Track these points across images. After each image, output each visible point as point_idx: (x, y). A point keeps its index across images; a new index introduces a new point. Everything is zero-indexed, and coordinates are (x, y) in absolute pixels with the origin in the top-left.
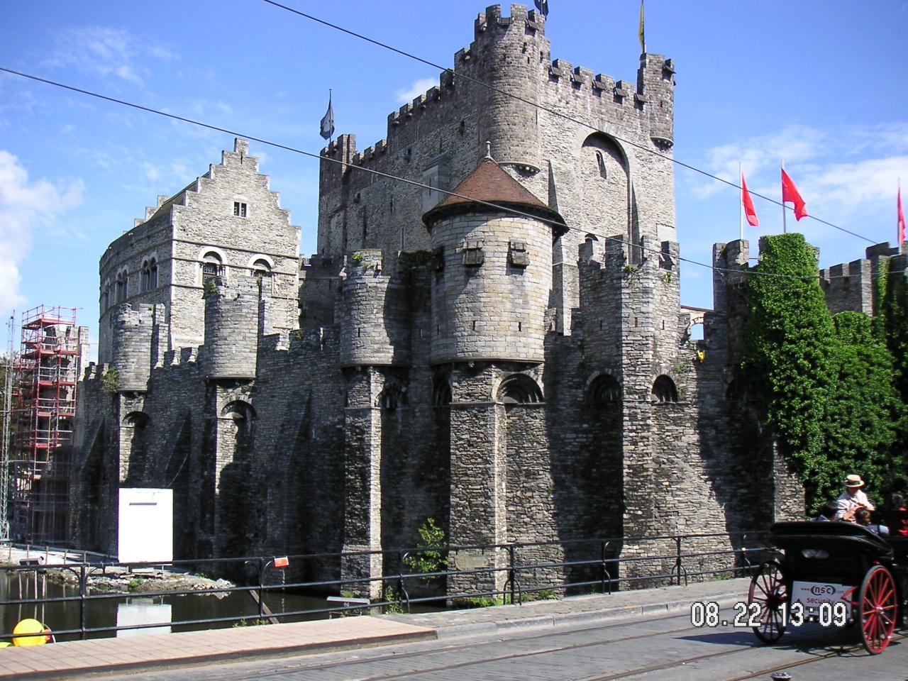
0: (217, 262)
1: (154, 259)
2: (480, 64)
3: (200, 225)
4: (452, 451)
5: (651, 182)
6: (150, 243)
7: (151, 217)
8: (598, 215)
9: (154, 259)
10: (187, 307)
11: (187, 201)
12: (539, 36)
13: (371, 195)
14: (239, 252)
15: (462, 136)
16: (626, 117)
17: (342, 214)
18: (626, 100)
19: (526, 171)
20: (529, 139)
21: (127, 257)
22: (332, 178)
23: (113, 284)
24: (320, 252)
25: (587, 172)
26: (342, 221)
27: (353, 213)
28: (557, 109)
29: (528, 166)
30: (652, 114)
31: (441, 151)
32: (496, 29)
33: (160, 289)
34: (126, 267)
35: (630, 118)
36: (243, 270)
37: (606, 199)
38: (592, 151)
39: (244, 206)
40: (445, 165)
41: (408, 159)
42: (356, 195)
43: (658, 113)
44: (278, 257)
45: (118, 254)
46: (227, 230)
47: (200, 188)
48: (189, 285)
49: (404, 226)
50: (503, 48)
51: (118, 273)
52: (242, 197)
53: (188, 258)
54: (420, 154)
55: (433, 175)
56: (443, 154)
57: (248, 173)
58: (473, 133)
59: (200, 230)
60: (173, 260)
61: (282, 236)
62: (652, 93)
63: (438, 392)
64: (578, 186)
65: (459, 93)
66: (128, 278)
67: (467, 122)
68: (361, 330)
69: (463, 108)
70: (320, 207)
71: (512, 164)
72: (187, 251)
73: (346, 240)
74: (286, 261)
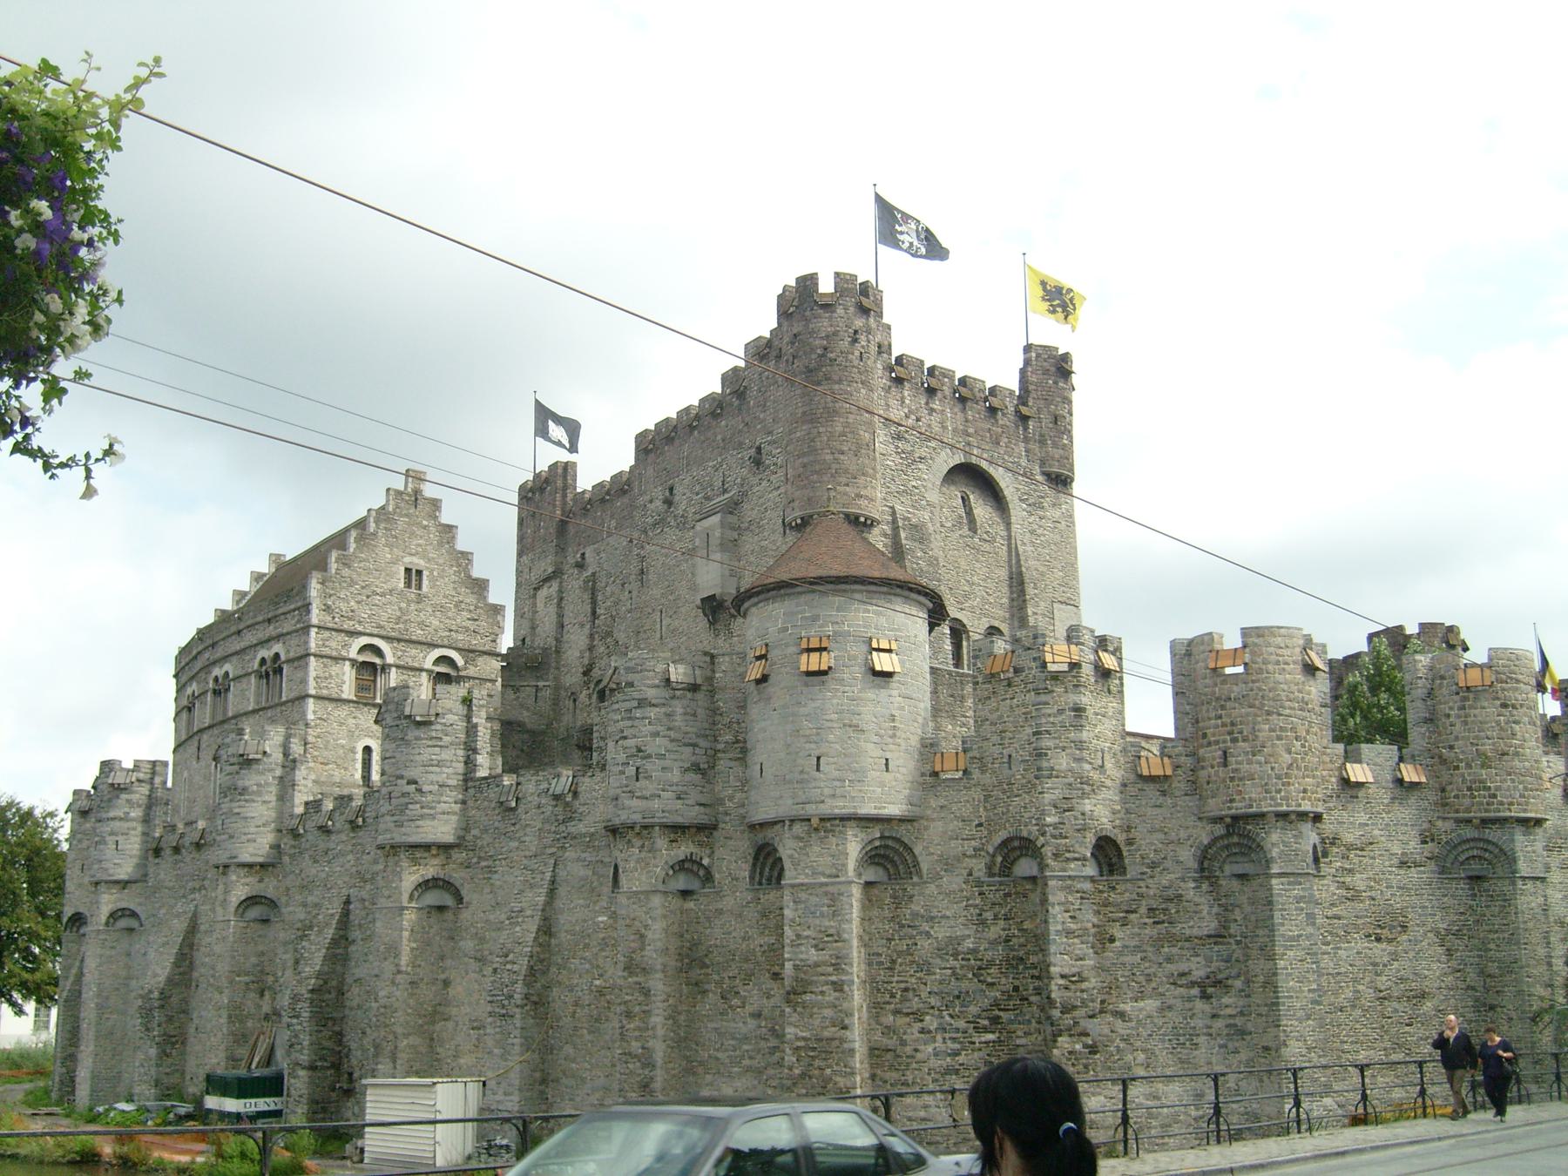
0: (377, 661)
1: (277, 656)
2: (787, 361)
3: (352, 604)
4: (786, 956)
5: (1042, 538)
6: (271, 630)
7: (258, 587)
8: (966, 588)
9: (277, 656)
10: (332, 731)
11: (333, 566)
12: (875, 320)
13: (603, 555)
14: (411, 646)
15: (758, 469)
16: (1004, 441)
17: (555, 585)
18: (1004, 414)
19: (859, 523)
20: (863, 474)
21: (230, 652)
23: (207, 691)
24: (519, 643)
25: (949, 525)
27: (574, 583)
28: (902, 428)
29: (863, 515)
30: (1042, 435)
31: (725, 491)
32: (812, 310)
33: (287, 702)
34: (227, 667)
35: (1010, 442)
37: (978, 565)
38: (955, 493)
39: (419, 573)
40: (731, 513)
41: (669, 502)
42: (579, 555)
43: (1052, 434)
44: (468, 652)
45: (213, 645)
46: (392, 611)
47: (352, 546)
48: (335, 696)
51: (214, 674)
52: (415, 560)
53: (334, 654)
56: (726, 496)
57: (425, 523)
59: (352, 611)
60: (312, 658)
62: (1041, 404)
63: (759, 864)
64: (936, 544)
66: (232, 684)
67: (766, 448)
68: (640, 770)
69: (759, 426)
70: (519, 573)
72: (333, 644)
73: (561, 626)
74: (481, 660)
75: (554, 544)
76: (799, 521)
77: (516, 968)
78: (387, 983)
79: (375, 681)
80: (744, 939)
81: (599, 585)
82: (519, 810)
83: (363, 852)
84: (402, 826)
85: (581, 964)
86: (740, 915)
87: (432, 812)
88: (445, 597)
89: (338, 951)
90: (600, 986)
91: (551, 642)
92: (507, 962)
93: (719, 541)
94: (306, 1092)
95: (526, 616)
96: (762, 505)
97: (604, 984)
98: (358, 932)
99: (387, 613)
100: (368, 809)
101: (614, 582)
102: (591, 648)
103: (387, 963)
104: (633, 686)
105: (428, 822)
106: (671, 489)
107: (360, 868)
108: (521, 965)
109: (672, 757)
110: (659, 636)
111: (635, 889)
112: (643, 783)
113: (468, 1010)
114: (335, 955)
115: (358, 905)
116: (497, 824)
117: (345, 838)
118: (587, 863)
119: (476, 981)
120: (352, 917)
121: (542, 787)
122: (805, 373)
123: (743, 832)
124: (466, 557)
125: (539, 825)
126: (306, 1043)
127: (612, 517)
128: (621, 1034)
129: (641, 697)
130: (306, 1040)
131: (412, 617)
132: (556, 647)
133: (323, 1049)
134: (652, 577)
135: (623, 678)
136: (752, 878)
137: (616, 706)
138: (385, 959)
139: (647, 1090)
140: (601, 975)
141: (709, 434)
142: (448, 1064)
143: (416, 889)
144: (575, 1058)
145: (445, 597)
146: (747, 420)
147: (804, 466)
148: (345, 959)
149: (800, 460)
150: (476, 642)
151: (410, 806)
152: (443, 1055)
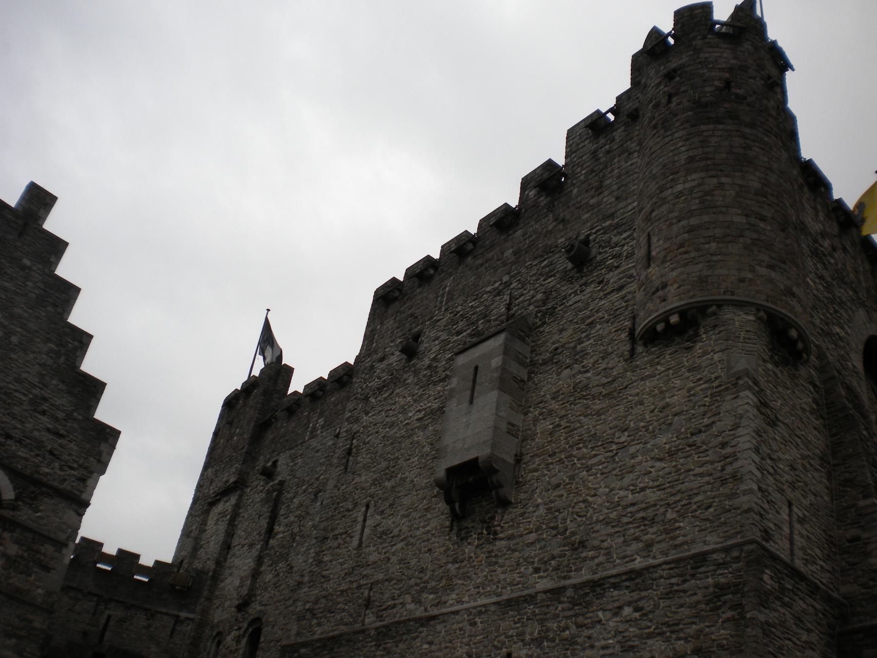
15: (580, 271)
17: (233, 500)
22: (232, 438)
26: (230, 509)
29: (798, 327)
42: (269, 464)
49: (372, 496)
50: (722, 70)
54: (444, 336)
57: (27, 262)
58: (617, 256)
61: (61, 436)
65: (575, 191)
70: (200, 487)
71: (759, 308)
73: (227, 547)
75: (244, 450)
88: (18, 380)
91: (211, 565)
93: (496, 375)
95: (193, 535)
96: (583, 320)
101: (305, 491)
102: (256, 574)
106: (416, 337)
110: (355, 542)
124: (82, 340)
127: (320, 416)
132: (215, 571)
134: (363, 458)
145: (18, 380)
146: (561, 217)
147: (691, 230)
149: (684, 223)
150: (48, 470)
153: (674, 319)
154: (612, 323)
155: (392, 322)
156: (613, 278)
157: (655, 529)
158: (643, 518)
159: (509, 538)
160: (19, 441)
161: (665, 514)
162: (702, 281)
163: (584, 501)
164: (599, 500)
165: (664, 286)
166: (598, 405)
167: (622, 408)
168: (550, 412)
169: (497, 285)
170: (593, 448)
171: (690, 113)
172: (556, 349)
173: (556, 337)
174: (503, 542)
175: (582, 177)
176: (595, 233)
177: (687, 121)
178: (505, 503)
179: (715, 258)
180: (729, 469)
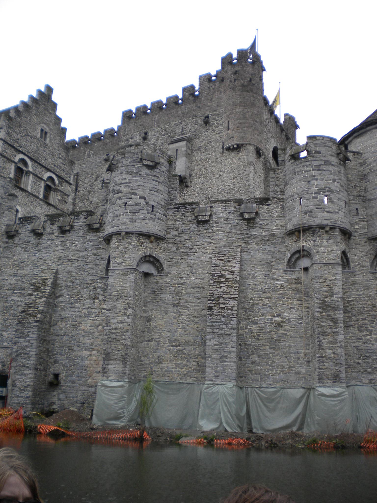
0: (24, 168)
3: (19, 136)
15: (206, 125)
31: (183, 134)
36: (40, 180)
39: (46, 133)
40: (189, 142)
41: (145, 139)
55: (182, 147)
56: (184, 136)
57: (50, 111)
59: (18, 140)
61: (64, 165)
65: (203, 99)
67: (211, 117)
72: (9, 152)
74: (65, 184)
76: (235, 146)
77: (230, 306)
78: (118, 315)
79: (21, 178)
80: (369, 299)
81: (80, 178)
82: (211, 222)
83: (71, 245)
84: (135, 221)
85: (264, 308)
86: (366, 286)
87: (154, 217)
88: (54, 149)
89: (51, 301)
90: (279, 321)
92: (220, 304)
93: (184, 153)
94: (32, 384)
96: (208, 140)
97: (281, 320)
98: (65, 291)
99: (32, 148)
100: (76, 221)
101: (90, 177)
103: (118, 302)
104: (320, 153)
105: (151, 222)
106: (146, 133)
107: (68, 254)
108: (234, 305)
109: (342, 194)
111: (325, 262)
112: (330, 204)
113: (168, 335)
114: (49, 303)
115: (65, 274)
116: (192, 229)
117: (54, 237)
118: (266, 252)
119: (174, 318)
120: (59, 282)
121: (229, 209)
122: (239, 86)
123: (365, 242)
125: (229, 230)
126: (35, 353)
127: (91, 150)
128: (319, 345)
129: (326, 159)
130: (33, 353)
131: (41, 152)
133: (41, 358)
135: (313, 149)
136: (371, 266)
137: (308, 163)
138: (117, 300)
139: (338, 379)
140: (279, 315)
141: (173, 111)
142: (151, 367)
143: (140, 261)
144: (259, 363)
145: (54, 149)
146: (198, 106)
147: (240, 123)
148: (55, 306)
149: (238, 121)
150: (63, 175)
151: (141, 211)
152: (147, 362)
153: (235, 146)
154: (217, 143)
155: (133, 125)
156: (217, 130)
157: (230, 195)
158: (227, 192)
159: (189, 195)
160: (57, 167)
161: (232, 191)
162: (243, 138)
163: (211, 187)
164: (215, 188)
165: (233, 137)
166: (213, 164)
167: (220, 166)
168: (199, 164)
169: (177, 122)
170: (213, 175)
171: (241, 87)
172: (200, 147)
173: (199, 143)
174: (188, 196)
175: (205, 94)
176: (211, 115)
177: (240, 90)
178: (187, 187)
179: (246, 132)
180: (247, 183)
